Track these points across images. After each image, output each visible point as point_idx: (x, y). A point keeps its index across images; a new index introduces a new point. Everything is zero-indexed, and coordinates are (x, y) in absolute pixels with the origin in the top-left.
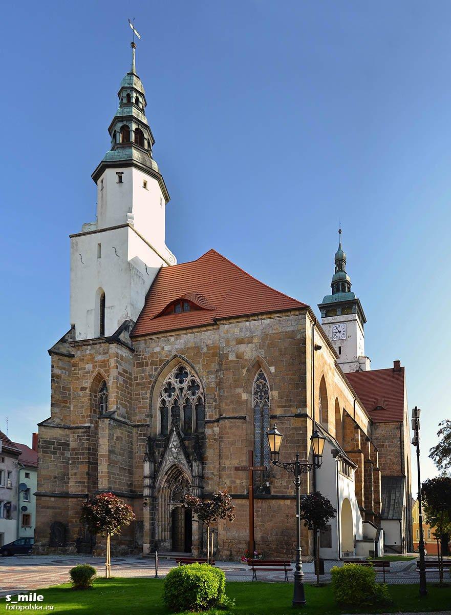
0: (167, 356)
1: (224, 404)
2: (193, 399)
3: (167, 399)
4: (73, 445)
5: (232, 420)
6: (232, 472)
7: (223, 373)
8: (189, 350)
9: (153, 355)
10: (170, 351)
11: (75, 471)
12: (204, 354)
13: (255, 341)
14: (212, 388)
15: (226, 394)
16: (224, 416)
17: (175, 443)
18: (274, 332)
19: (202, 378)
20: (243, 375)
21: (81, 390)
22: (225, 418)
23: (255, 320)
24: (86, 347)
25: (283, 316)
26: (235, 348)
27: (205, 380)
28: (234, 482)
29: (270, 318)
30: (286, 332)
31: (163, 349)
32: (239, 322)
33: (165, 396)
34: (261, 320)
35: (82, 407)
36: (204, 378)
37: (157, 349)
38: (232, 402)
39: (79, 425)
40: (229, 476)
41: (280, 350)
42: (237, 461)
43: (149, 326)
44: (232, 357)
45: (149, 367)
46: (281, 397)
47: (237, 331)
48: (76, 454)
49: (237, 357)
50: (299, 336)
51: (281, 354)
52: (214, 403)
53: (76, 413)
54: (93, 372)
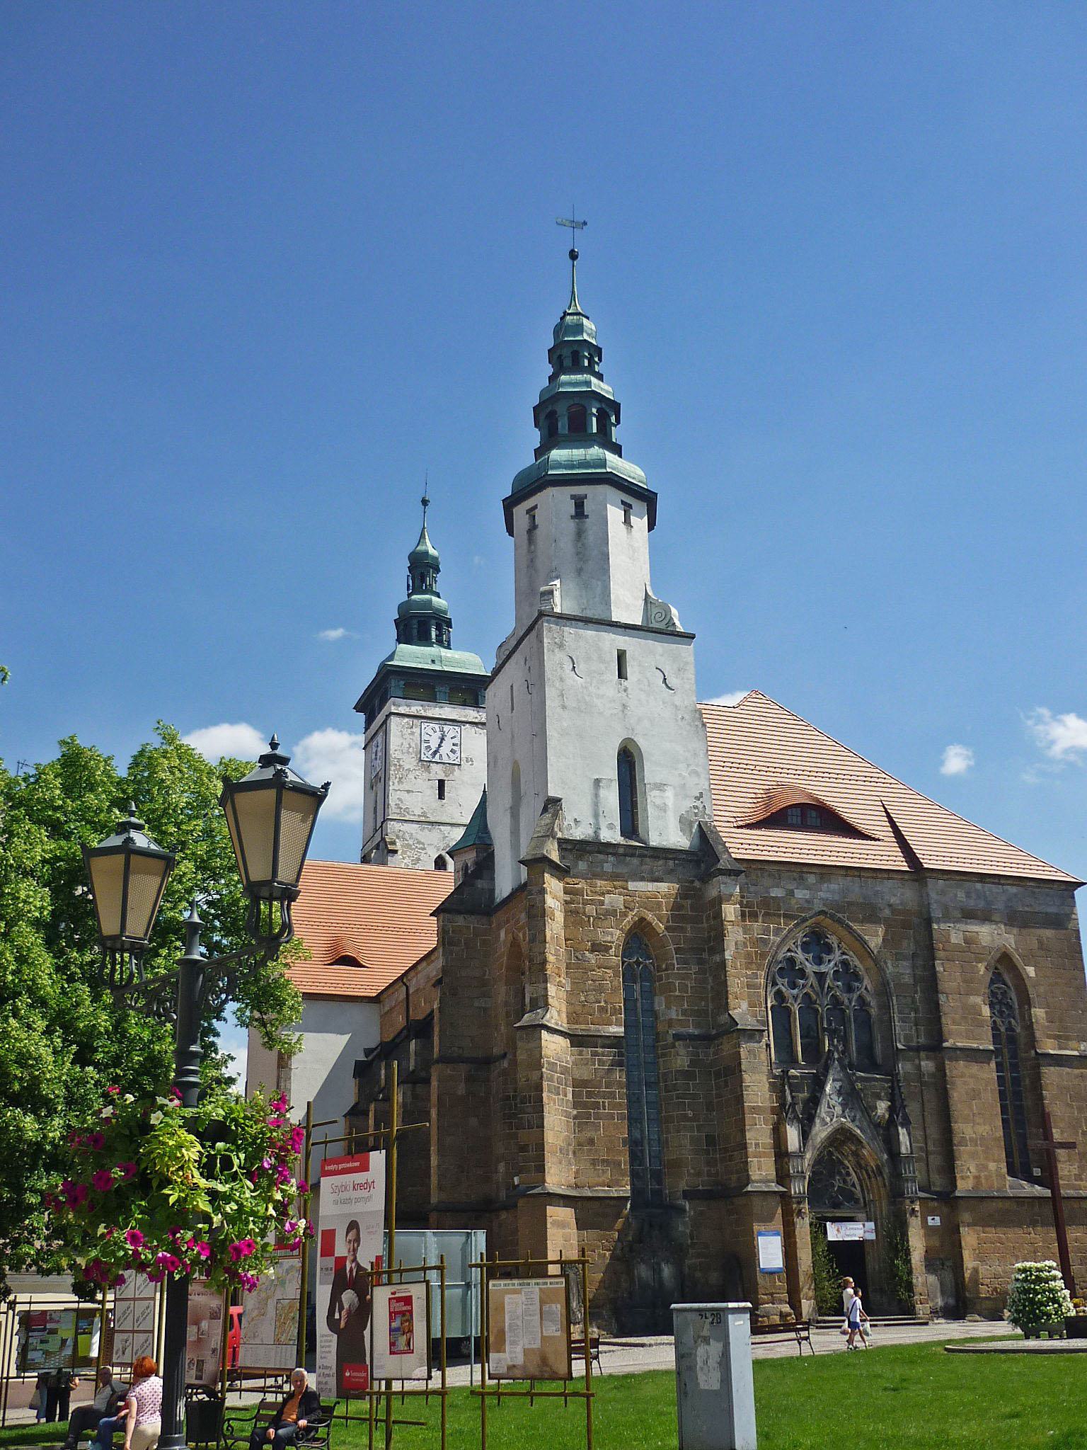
0: (802, 909)
2: (850, 1002)
7: (942, 964)
10: (807, 901)
18: (1026, 909)
19: (886, 963)
20: (981, 973)
21: (592, 951)
23: (993, 883)
24: (601, 857)
25: (1039, 887)
27: (890, 967)
28: (985, 1167)
29: (1018, 885)
30: (1046, 913)
31: (791, 893)
32: (963, 880)
34: (1003, 885)
36: (889, 965)
37: (776, 892)
40: (973, 1155)
47: (961, 895)
48: (589, 1095)
49: (967, 941)
52: (913, 1015)
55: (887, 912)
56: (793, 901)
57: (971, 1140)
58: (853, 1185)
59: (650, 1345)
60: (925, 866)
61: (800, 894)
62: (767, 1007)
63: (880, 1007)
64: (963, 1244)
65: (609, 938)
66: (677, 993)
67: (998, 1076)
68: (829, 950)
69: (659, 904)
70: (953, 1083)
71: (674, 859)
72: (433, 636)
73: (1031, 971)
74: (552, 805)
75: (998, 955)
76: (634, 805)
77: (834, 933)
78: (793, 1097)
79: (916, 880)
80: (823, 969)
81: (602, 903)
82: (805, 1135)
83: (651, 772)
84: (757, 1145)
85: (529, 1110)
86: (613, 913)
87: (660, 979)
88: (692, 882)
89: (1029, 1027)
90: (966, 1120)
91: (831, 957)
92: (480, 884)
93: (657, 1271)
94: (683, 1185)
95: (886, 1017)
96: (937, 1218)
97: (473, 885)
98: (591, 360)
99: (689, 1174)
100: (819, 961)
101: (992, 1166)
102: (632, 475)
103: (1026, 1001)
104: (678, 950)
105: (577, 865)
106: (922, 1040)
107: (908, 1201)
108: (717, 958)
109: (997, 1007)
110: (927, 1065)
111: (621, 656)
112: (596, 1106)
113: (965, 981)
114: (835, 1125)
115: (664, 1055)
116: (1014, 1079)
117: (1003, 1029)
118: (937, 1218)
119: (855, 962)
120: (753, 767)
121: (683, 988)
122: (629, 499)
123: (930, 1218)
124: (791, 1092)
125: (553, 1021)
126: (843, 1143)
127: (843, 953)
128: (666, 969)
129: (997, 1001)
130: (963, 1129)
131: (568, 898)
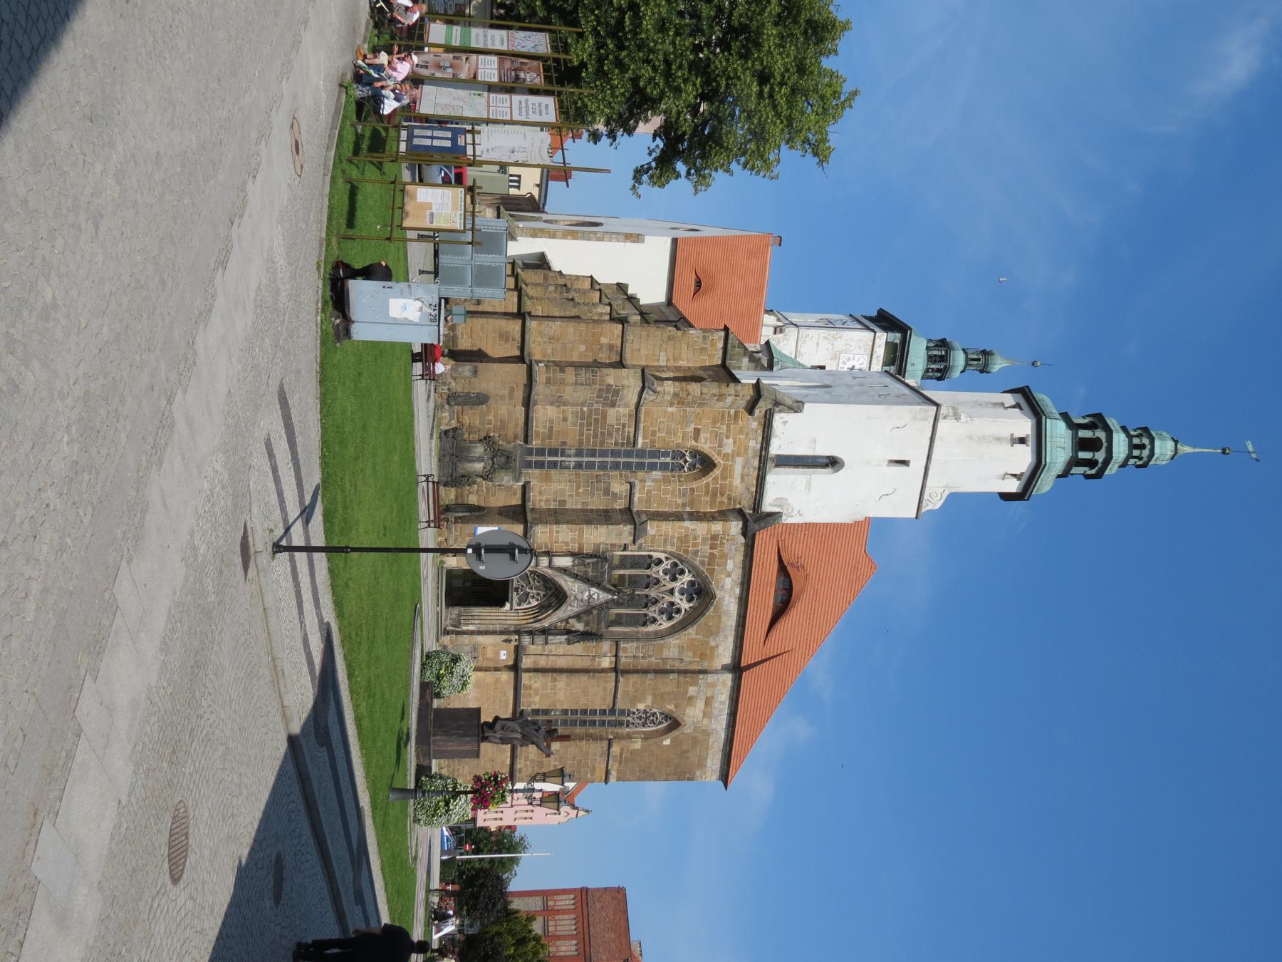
1: (635, 680)
3: (661, 568)
4: (612, 413)
5: (613, 691)
6: (549, 691)
8: (717, 619)
9: (724, 557)
10: (723, 587)
11: (570, 420)
12: (707, 642)
13: (705, 722)
14: (661, 654)
15: (648, 682)
16: (621, 679)
17: (595, 596)
20: (667, 706)
22: (617, 682)
24: (760, 439)
26: (702, 694)
28: (536, 694)
30: (706, 758)
31: (729, 575)
33: (667, 565)
35: (669, 432)
38: (637, 691)
39: (641, 425)
40: (544, 687)
41: (687, 751)
42: (562, 698)
43: (765, 541)
44: (692, 690)
45: (709, 551)
46: (633, 752)
48: (596, 420)
49: (691, 698)
50: (698, 773)
51: (682, 752)
52: (641, 655)
53: (662, 419)
54: (719, 454)
55: (713, 643)
56: (723, 576)
57: (555, 686)
58: (529, 603)
59: (430, 443)
60: (744, 674)
61: (728, 582)
62: (650, 551)
63: (648, 633)
64: (488, 673)
65: (703, 441)
66: (663, 487)
67: (596, 710)
68: (690, 600)
69: (724, 478)
70: (593, 678)
71: (756, 492)
72: (933, 366)
73: (667, 742)
74: (796, 407)
75: (680, 721)
76: (796, 466)
77: (700, 605)
78: (589, 563)
79: (734, 667)
80: (677, 594)
81: (728, 437)
82: (564, 571)
83: (821, 477)
84: (558, 532)
85: (588, 375)
86: (720, 446)
87: (673, 476)
88: (740, 504)
89: (629, 736)
90: (567, 685)
91: (684, 601)
92: (745, 360)
93: (480, 459)
94: (534, 482)
95: (640, 636)
96: (504, 658)
97: (745, 355)
98: (1140, 458)
99: (540, 486)
100: (682, 592)
101: (537, 699)
102: (1044, 482)
103: (647, 737)
104: (692, 490)
105: (755, 421)
106: (623, 660)
107: (517, 637)
108: (685, 516)
109: (644, 716)
110: (606, 663)
111: (904, 463)
112: (589, 425)
113: (662, 694)
114: (568, 593)
115: (621, 475)
116: (595, 721)
117: (629, 718)
118: (504, 658)
119: (678, 618)
120: (820, 558)
121: (666, 492)
122: (1025, 478)
123: (505, 652)
124: (593, 563)
125: (647, 396)
126: (557, 597)
127: (686, 610)
128: (679, 481)
129: (647, 717)
130: (562, 681)
131: (732, 412)
